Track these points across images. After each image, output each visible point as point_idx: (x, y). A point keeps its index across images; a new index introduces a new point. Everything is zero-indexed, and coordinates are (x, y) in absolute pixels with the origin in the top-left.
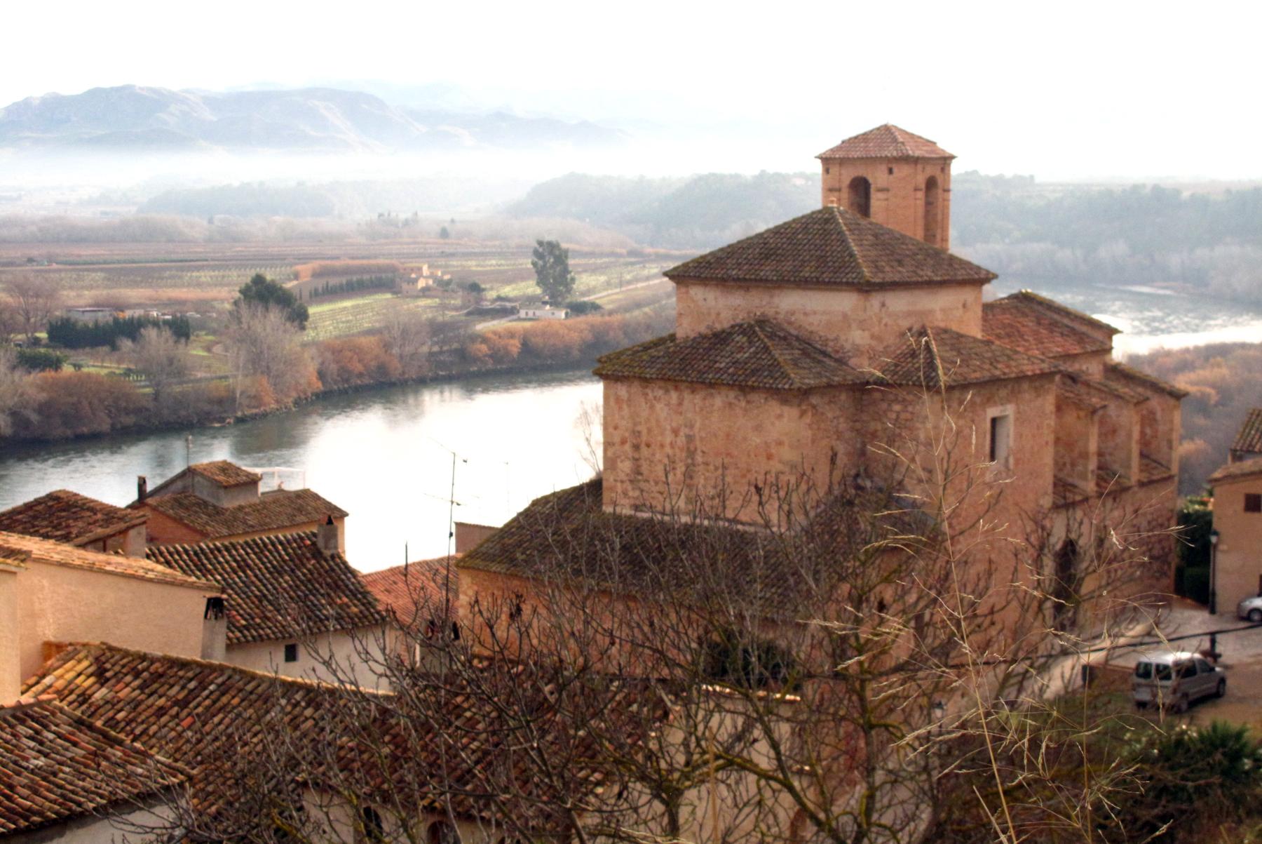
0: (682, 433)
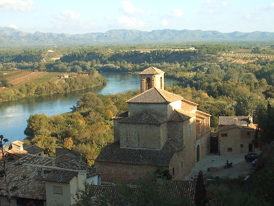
0: (136, 133)
